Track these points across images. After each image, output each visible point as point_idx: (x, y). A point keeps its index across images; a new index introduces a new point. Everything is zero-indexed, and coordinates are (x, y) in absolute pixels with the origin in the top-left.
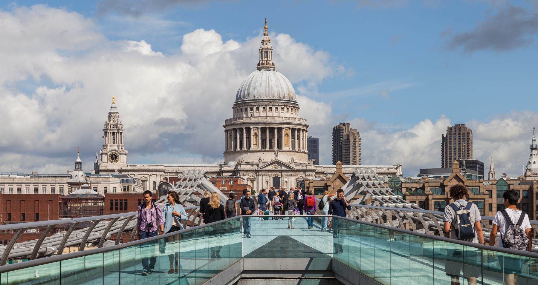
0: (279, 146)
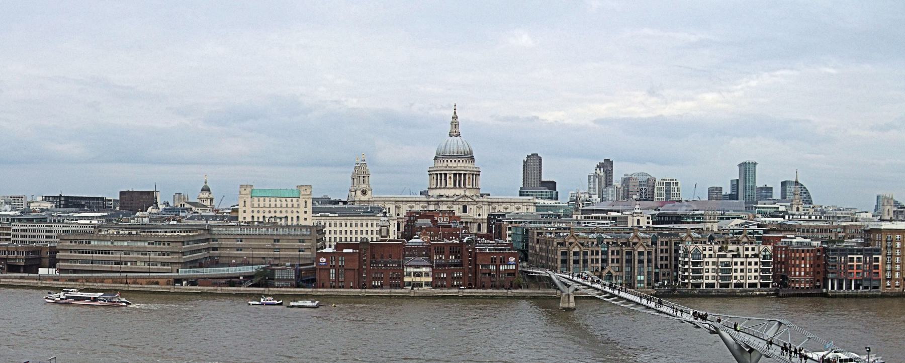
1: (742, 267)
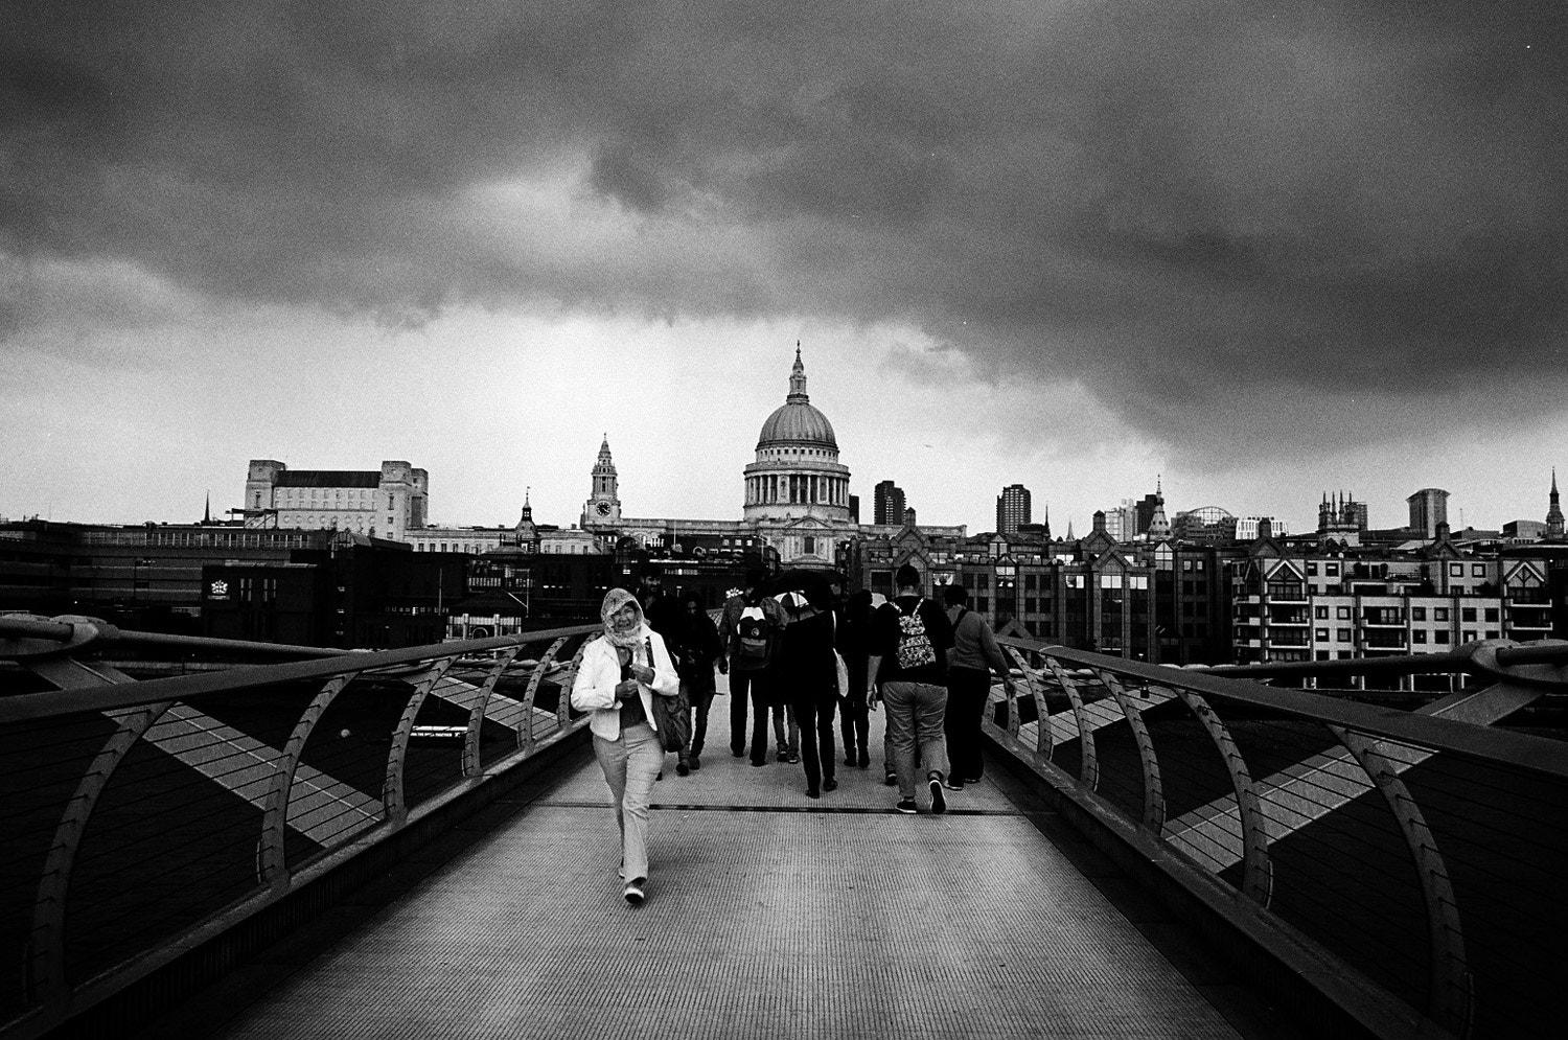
1: (1445, 626)
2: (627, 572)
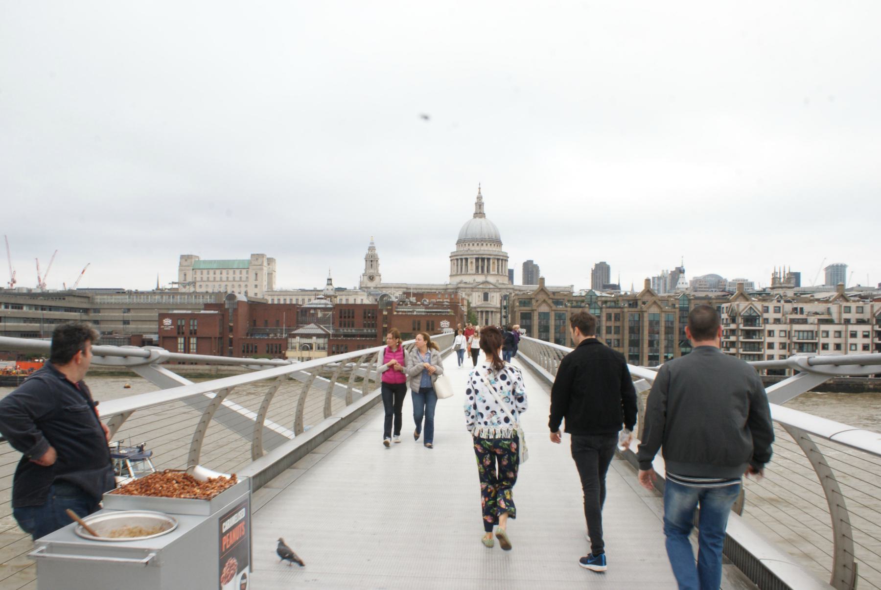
0: (488, 271)
1: (838, 341)
2: (385, 313)
